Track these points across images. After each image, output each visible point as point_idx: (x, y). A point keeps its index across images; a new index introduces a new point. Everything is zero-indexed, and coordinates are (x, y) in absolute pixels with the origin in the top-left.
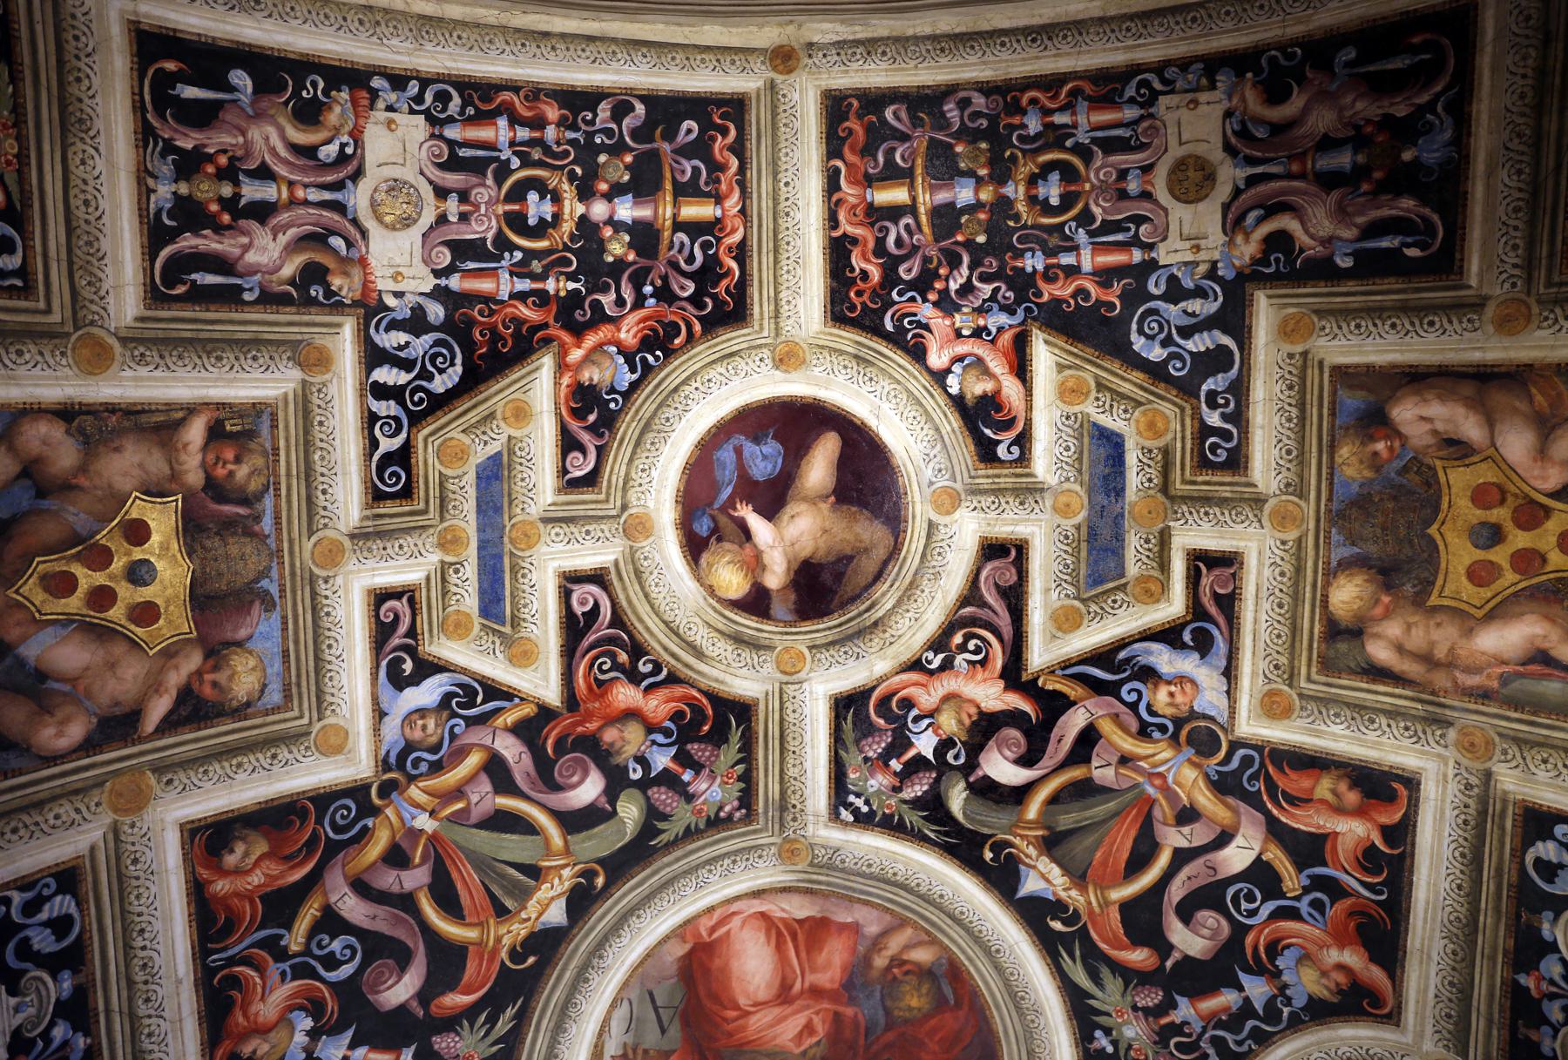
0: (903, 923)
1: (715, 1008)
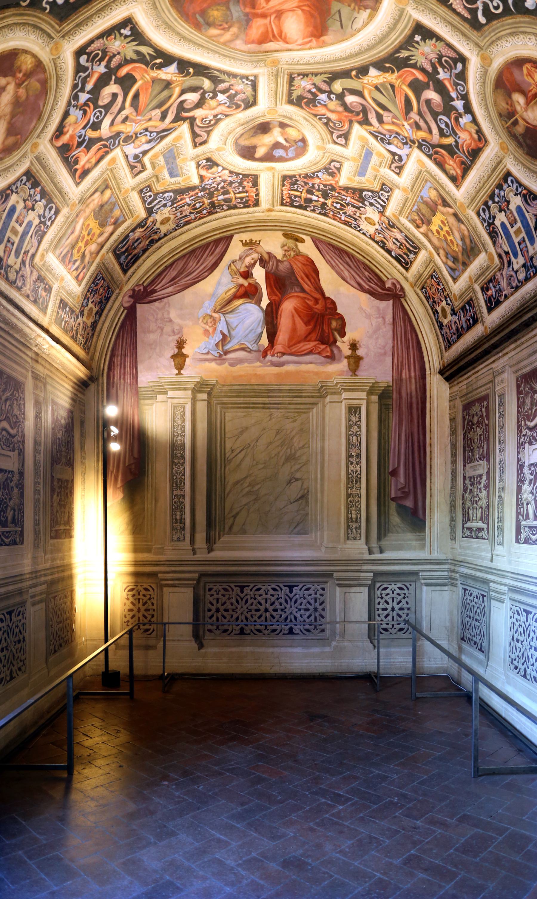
0: (224, 44)
1: (313, 12)
